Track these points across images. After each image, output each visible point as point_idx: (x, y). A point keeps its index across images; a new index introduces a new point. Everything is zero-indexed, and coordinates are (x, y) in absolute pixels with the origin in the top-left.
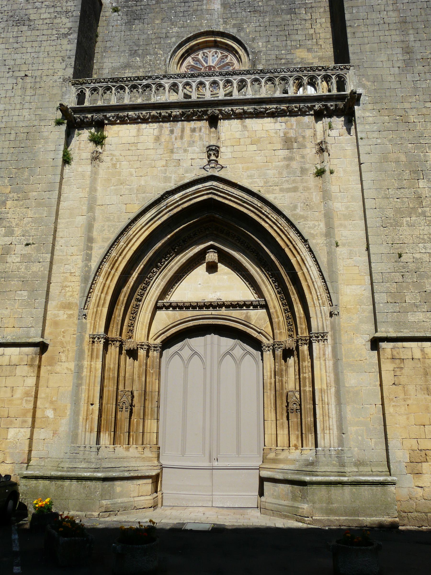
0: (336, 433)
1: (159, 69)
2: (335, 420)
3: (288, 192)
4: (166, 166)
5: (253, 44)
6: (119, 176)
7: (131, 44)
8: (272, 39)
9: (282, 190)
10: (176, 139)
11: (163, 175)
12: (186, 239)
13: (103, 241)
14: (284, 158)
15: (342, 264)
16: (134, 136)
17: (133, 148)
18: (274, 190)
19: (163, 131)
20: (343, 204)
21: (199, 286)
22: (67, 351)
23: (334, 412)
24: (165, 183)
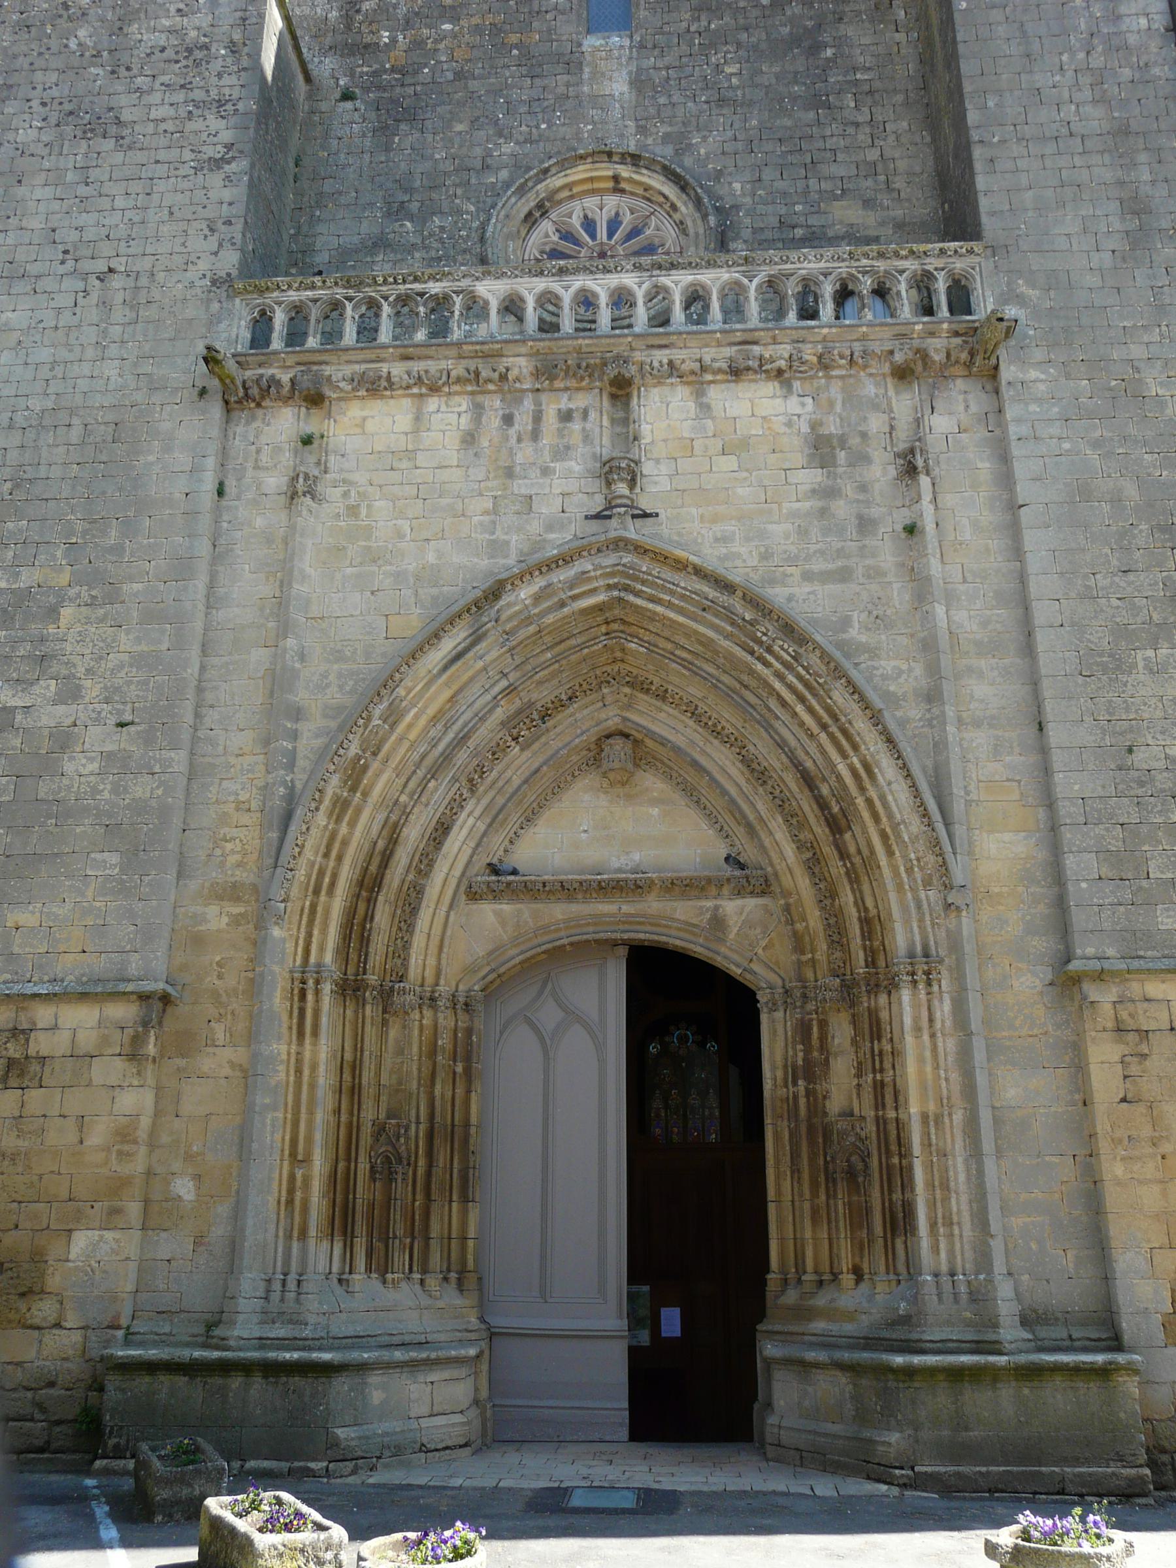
0: (971, 1234)
1: (465, 251)
2: (964, 1198)
3: (823, 583)
4: (495, 511)
5: (718, 187)
6: (368, 538)
7: (389, 185)
8: (768, 174)
9: (808, 577)
10: (519, 440)
11: (487, 536)
12: (548, 709)
13: (325, 716)
14: (814, 491)
15: (974, 776)
16: (406, 434)
17: (405, 464)
18: (787, 575)
19: (484, 419)
20: (972, 613)
21: (584, 835)
22: (229, 1017)
23: (962, 1177)
24: (493, 557)
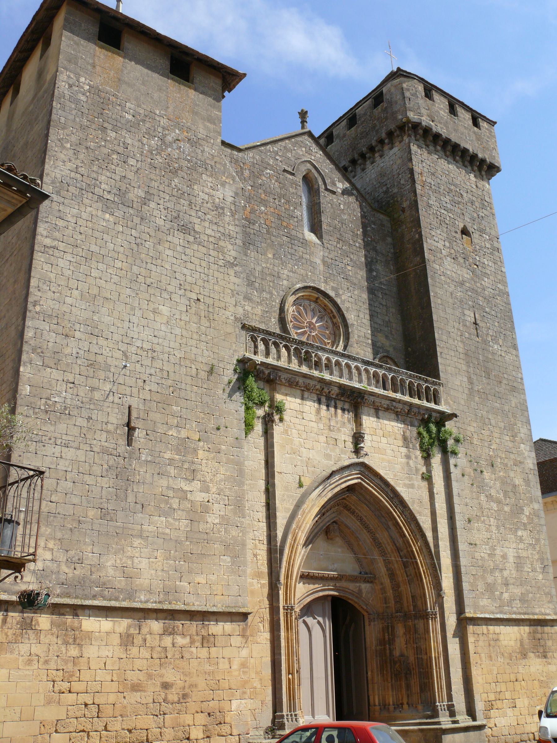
6: (292, 444)
